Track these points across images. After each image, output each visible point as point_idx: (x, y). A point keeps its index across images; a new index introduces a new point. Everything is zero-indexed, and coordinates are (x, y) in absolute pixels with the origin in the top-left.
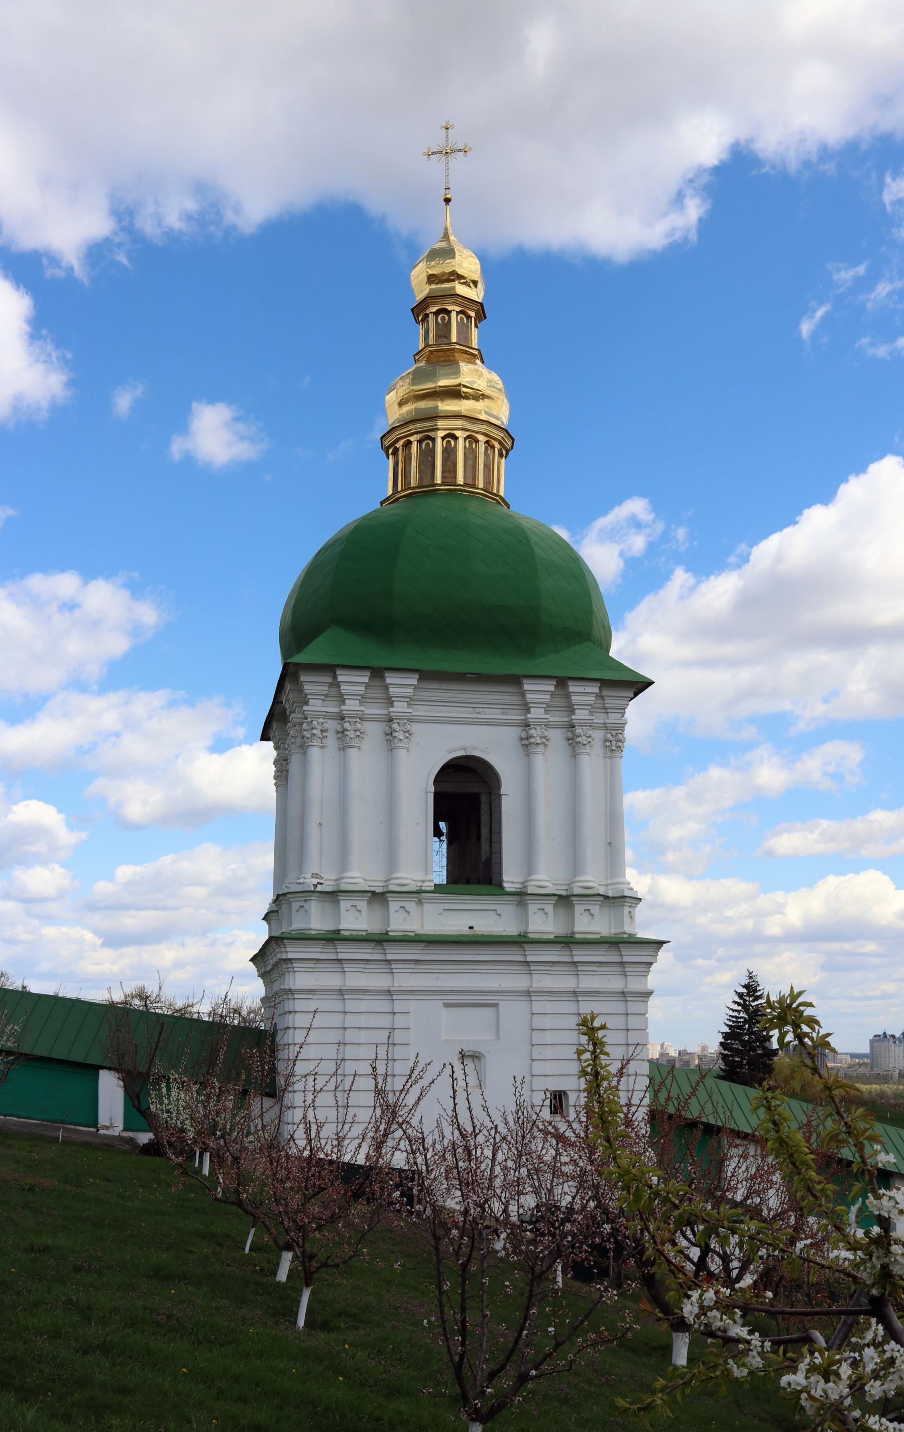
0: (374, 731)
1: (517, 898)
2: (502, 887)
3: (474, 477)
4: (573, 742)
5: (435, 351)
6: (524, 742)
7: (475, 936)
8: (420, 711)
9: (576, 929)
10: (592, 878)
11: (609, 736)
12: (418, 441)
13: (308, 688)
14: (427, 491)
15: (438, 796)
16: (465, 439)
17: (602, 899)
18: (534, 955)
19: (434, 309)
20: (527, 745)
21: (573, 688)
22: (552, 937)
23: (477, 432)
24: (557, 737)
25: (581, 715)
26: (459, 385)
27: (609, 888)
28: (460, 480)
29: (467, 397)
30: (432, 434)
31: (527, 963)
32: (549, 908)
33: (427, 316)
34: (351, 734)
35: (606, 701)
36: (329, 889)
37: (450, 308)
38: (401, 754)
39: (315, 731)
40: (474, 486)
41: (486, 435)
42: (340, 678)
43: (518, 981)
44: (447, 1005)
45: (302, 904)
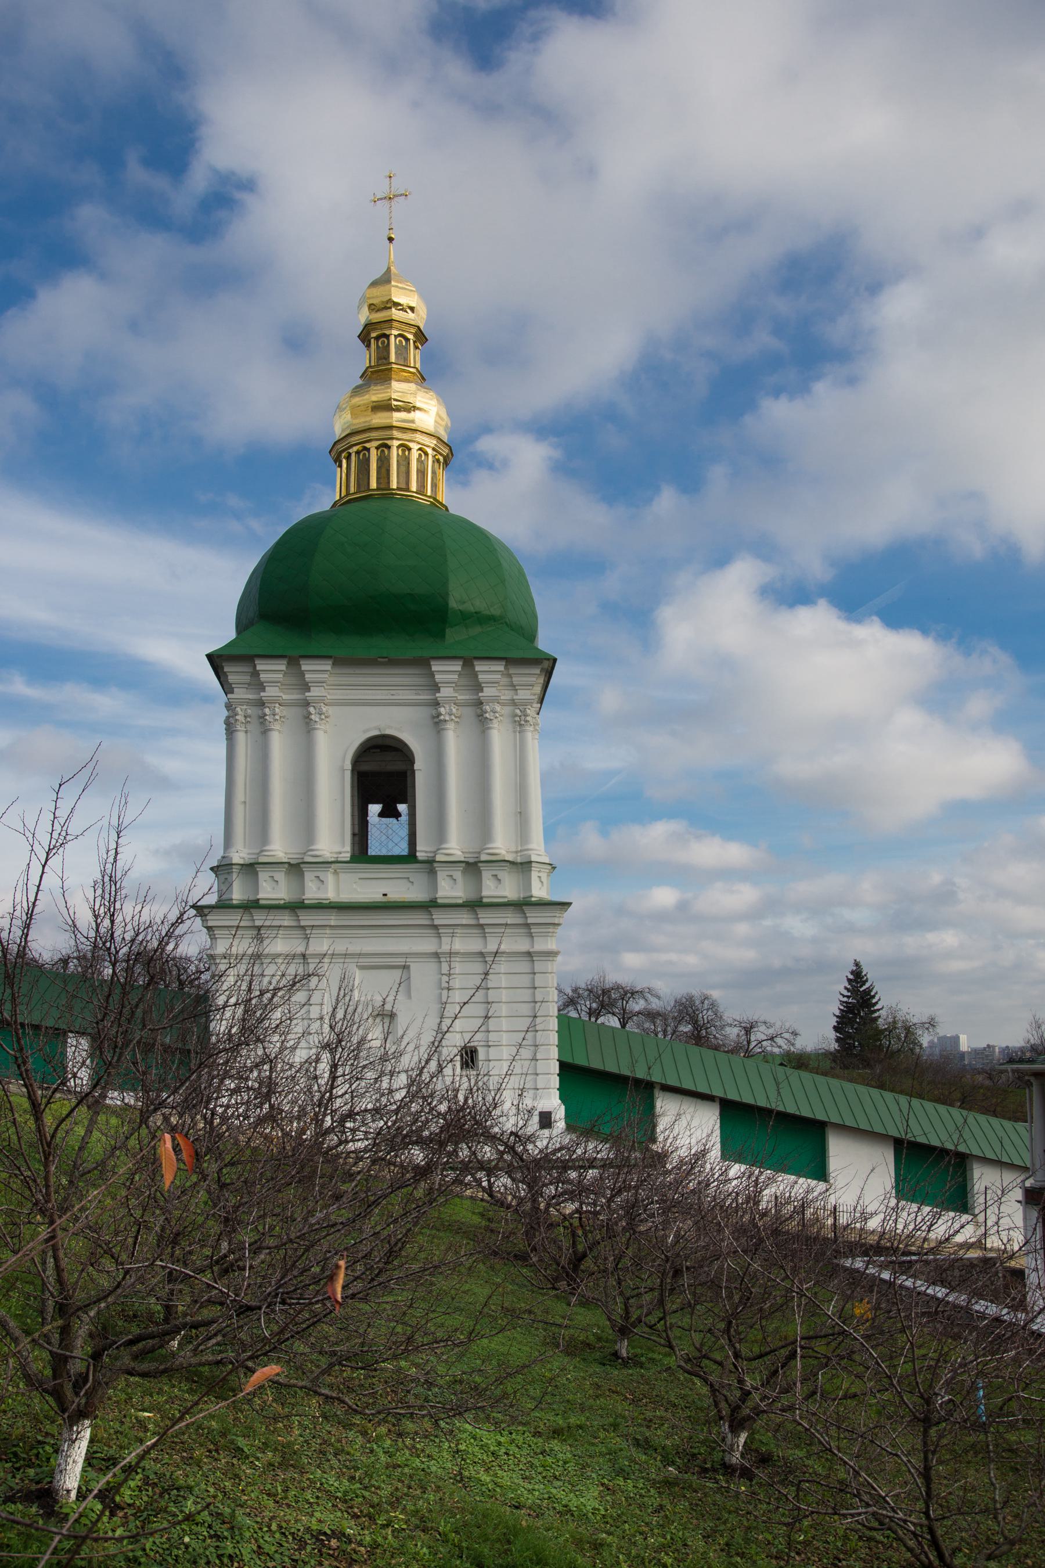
9: (484, 893)
10: (502, 845)
11: (518, 712)
16: (398, 447)
18: (440, 918)
21: (479, 666)
22: (460, 901)
23: (409, 441)
26: (390, 399)
29: (398, 409)
31: (482, 926)
32: (458, 875)
35: (514, 679)
37: (387, 332)
40: (408, 490)
42: (258, 668)
43: (427, 945)
44: (362, 968)
45: (226, 876)
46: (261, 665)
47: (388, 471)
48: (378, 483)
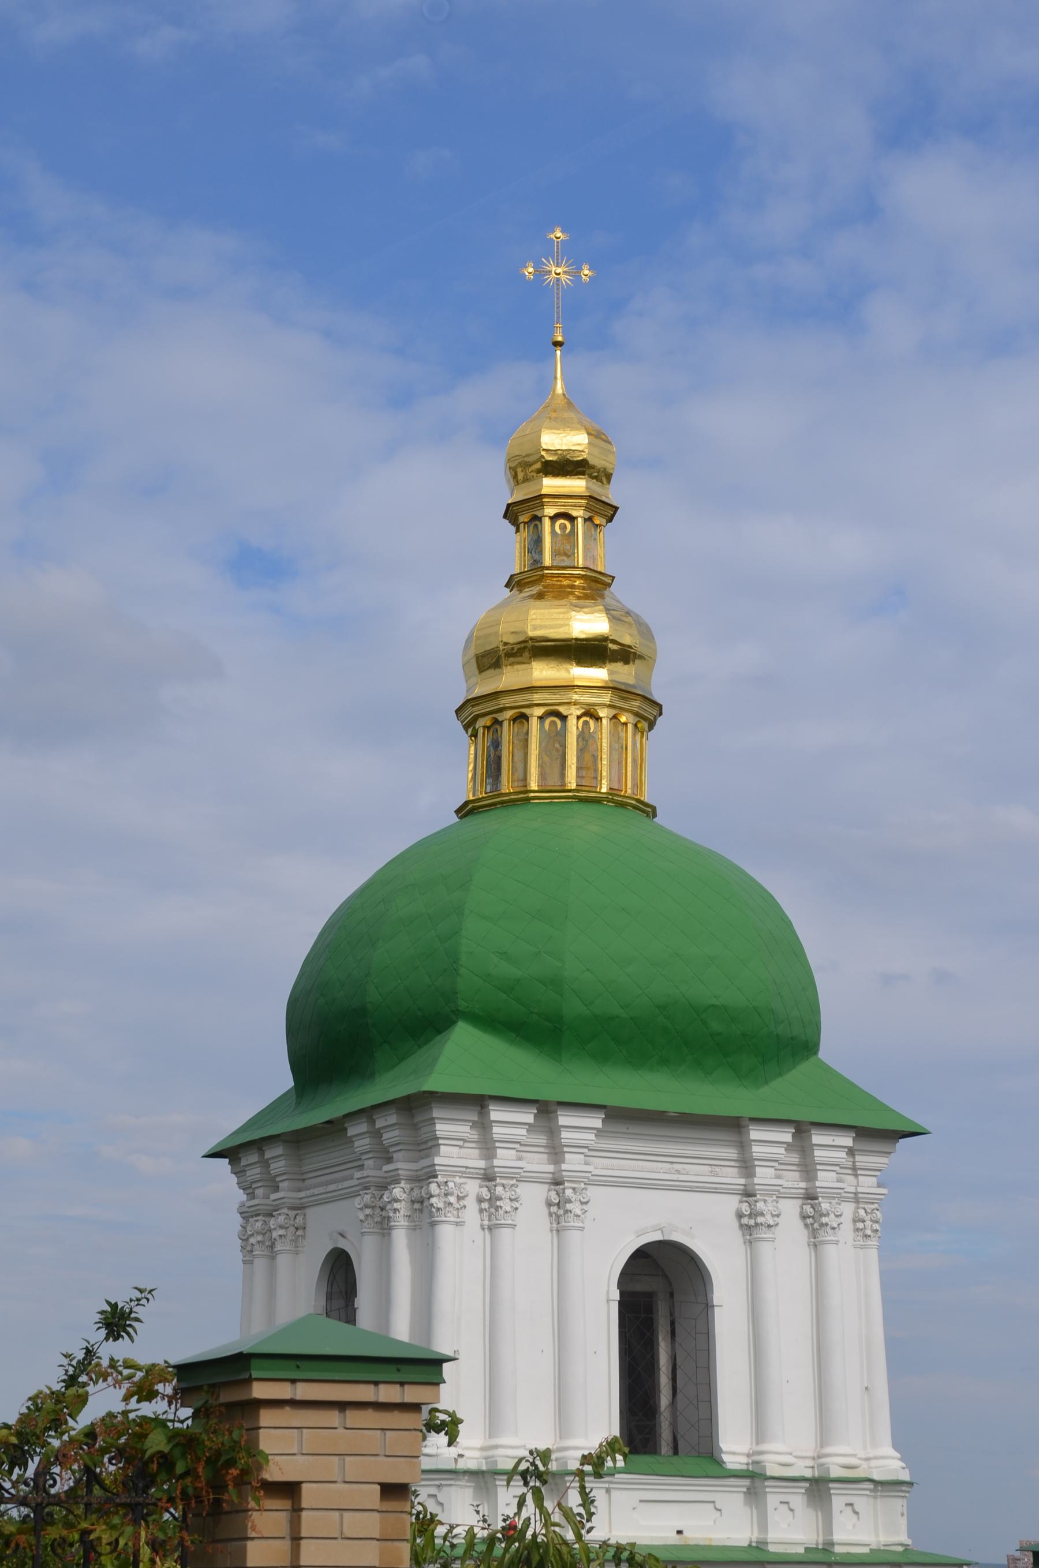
0: (534, 1197)
1: (747, 1482)
2: (720, 1463)
4: (814, 1224)
5: (553, 576)
6: (745, 1221)
7: (687, 1547)
8: (600, 1166)
11: (862, 1212)
12: (540, 718)
13: (442, 1128)
15: (622, 1304)
17: (871, 1486)
19: (550, 511)
20: (750, 1227)
24: (790, 1209)
25: (825, 1179)
27: (873, 1463)
30: (562, 709)
33: (537, 519)
34: (506, 1205)
36: (472, 1465)
37: (574, 513)
38: (573, 1237)
39: (452, 1199)
41: (637, 714)
45: (433, 1491)
46: (497, 1113)
47: (595, 758)
48: (579, 777)
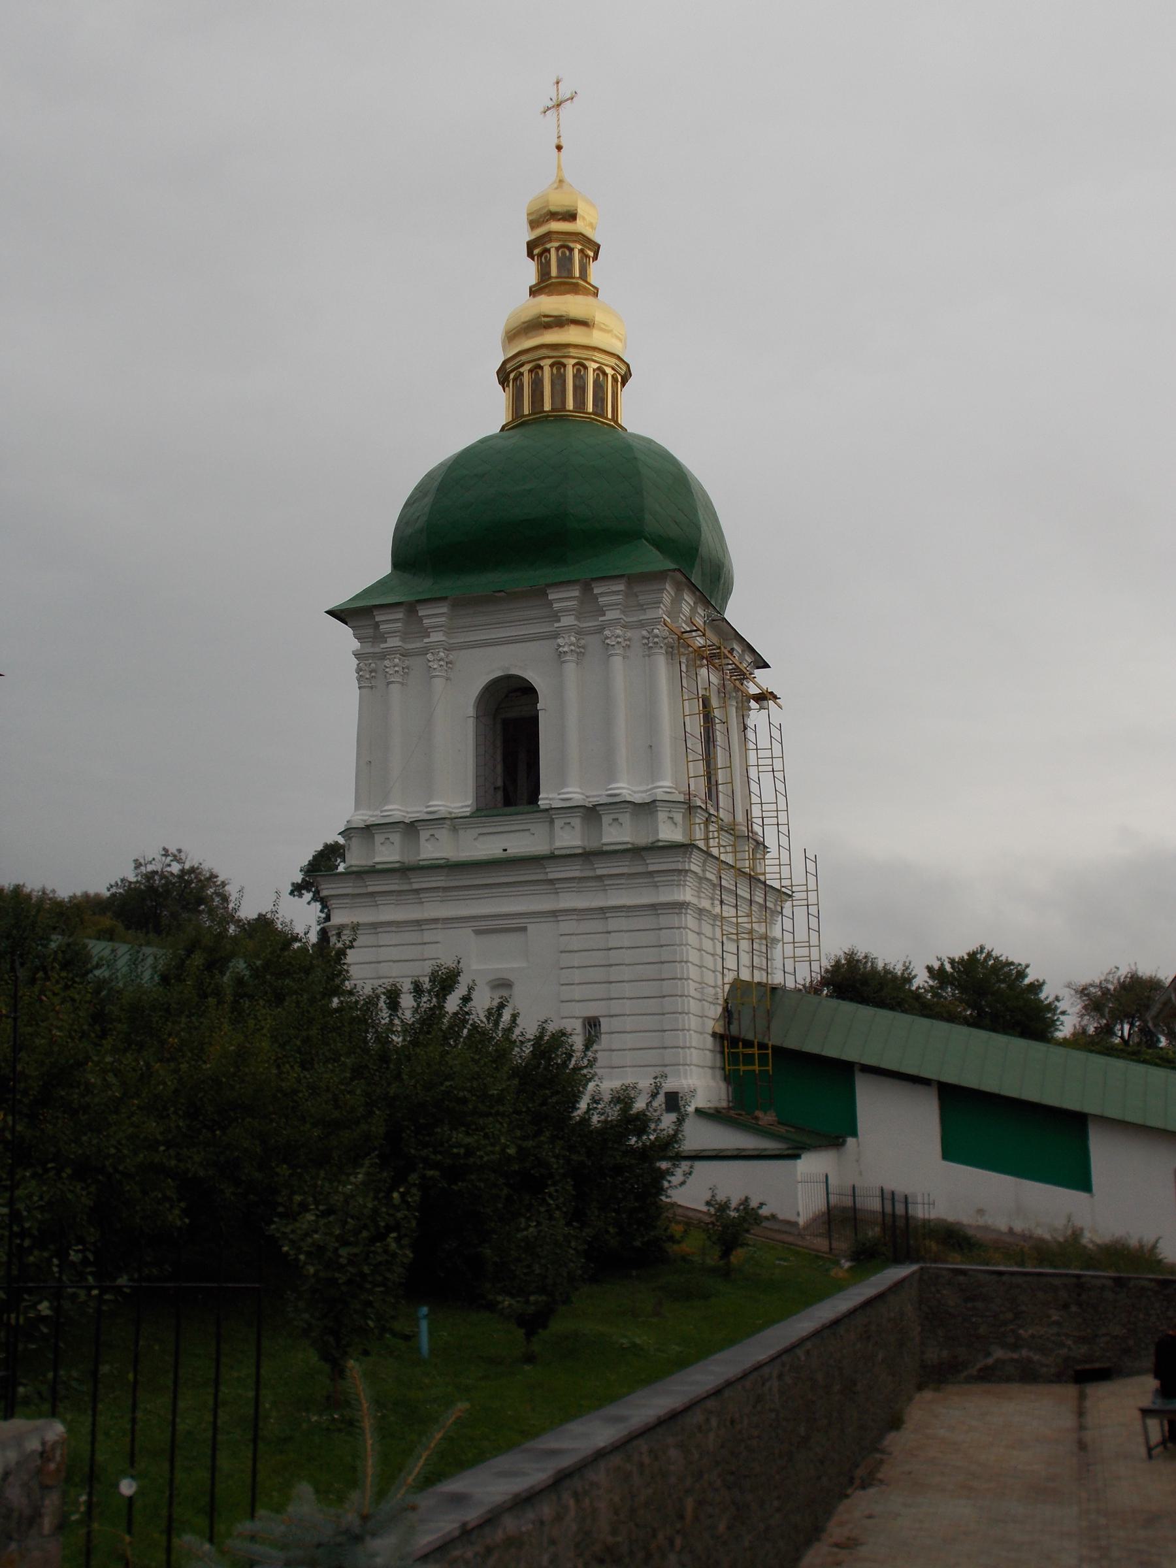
3: (564, 401)
14: (539, 418)
28: (547, 407)
40: (564, 408)
